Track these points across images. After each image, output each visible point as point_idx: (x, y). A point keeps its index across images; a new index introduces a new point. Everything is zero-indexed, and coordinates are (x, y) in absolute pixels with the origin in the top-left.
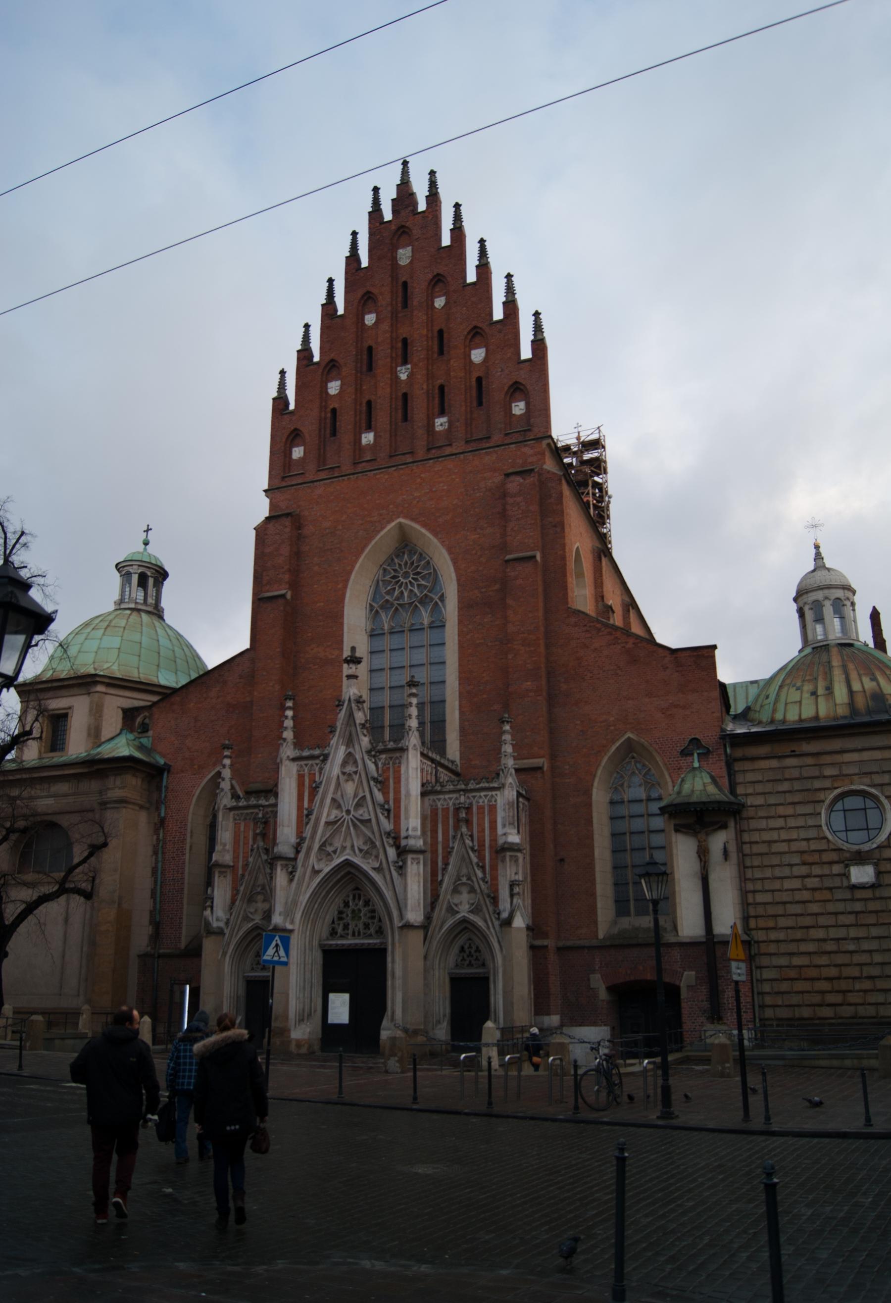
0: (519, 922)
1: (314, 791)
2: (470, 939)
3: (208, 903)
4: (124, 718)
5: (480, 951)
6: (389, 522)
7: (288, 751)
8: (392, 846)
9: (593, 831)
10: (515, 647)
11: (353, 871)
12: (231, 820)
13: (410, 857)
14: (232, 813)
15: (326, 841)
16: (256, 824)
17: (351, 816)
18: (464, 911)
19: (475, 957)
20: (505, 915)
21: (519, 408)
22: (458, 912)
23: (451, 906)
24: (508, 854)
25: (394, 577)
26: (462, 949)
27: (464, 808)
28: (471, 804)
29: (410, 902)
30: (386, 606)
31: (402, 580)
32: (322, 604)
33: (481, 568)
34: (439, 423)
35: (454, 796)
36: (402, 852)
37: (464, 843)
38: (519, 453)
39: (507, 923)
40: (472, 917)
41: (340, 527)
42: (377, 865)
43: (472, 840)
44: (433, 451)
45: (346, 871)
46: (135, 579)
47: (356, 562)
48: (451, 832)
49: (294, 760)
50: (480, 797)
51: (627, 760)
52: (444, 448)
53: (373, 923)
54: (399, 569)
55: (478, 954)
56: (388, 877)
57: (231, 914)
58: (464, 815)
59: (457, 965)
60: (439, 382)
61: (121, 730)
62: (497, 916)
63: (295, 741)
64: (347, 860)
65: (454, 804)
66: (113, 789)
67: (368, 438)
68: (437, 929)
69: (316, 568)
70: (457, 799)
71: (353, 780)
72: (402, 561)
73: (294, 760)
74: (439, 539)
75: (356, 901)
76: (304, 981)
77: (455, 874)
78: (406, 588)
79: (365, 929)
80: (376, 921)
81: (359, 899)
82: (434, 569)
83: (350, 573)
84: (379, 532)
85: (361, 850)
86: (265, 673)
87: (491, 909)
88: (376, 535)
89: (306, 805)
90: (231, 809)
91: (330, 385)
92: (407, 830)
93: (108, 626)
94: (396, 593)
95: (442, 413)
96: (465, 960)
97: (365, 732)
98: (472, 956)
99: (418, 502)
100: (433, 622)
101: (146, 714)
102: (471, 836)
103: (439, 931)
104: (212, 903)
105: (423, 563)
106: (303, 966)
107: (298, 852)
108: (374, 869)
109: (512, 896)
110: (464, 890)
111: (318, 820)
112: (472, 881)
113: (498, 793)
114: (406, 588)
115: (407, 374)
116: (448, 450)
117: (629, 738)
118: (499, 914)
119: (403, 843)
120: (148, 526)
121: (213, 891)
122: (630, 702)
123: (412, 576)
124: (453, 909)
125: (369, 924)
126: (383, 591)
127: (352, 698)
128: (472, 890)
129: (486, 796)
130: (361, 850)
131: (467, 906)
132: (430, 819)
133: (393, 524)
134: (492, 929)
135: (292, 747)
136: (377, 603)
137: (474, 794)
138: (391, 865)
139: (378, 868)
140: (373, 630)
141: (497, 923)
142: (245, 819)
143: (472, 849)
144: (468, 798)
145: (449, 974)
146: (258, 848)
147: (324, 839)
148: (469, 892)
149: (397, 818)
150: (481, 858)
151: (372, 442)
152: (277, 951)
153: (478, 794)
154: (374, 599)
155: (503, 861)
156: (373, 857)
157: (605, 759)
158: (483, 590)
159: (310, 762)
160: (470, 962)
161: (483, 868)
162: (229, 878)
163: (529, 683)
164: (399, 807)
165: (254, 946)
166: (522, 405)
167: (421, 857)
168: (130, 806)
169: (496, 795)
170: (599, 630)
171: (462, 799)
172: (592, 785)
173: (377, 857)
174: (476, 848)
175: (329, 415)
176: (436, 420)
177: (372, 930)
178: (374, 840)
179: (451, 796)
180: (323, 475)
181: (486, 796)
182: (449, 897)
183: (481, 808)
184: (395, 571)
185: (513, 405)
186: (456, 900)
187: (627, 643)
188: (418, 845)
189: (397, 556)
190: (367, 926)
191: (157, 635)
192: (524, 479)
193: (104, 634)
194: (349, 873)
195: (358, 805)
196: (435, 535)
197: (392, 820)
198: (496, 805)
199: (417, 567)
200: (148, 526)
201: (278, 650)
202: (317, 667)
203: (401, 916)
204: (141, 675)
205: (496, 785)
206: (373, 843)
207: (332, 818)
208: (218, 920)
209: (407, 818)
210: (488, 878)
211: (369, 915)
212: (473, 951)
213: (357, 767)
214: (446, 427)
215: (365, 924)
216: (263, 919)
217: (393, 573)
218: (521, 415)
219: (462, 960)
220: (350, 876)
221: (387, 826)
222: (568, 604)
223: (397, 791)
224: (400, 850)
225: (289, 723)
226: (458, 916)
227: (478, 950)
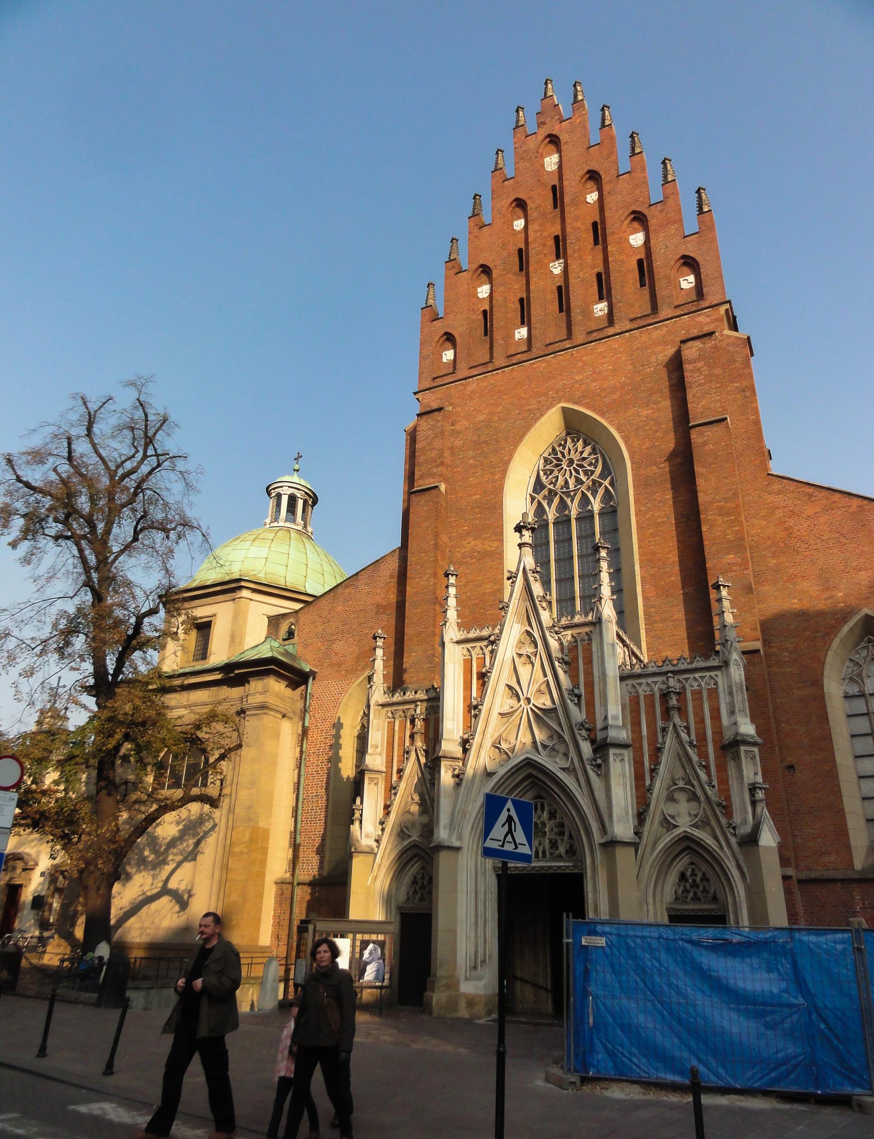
0: (768, 839)
1: (483, 677)
2: (692, 863)
3: (357, 815)
4: (269, 626)
5: (708, 880)
6: (548, 409)
7: (452, 633)
8: (586, 739)
9: (830, 730)
10: (709, 517)
11: (535, 773)
12: (384, 717)
13: (612, 751)
14: (386, 709)
15: (500, 736)
16: (413, 722)
17: (531, 705)
18: (684, 825)
19: (701, 888)
20: (747, 829)
21: (688, 282)
22: (675, 826)
23: (665, 818)
24: (743, 748)
25: (557, 466)
26: (683, 877)
27: (674, 693)
28: (684, 688)
29: (616, 811)
31: (568, 469)
32: (478, 496)
33: (658, 444)
34: (598, 310)
35: (660, 679)
36: (601, 747)
37: (678, 736)
38: (693, 323)
39: (751, 841)
40: (696, 833)
41: (496, 419)
42: (567, 765)
43: (689, 734)
44: (595, 334)
45: (526, 773)
46: (285, 500)
48: (660, 723)
49: (458, 642)
50: (695, 679)
51: (863, 644)
52: (606, 330)
53: (563, 840)
55: (705, 883)
56: (582, 779)
57: (383, 830)
58: (675, 702)
59: (677, 899)
60: (596, 270)
61: (266, 638)
62: (732, 831)
63: (459, 621)
64: (528, 758)
65: (661, 690)
66: (254, 694)
67: (522, 333)
68: (648, 849)
69: (471, 462)
70: (663, 683)
71: (532, 663)
72: (564, 449)
73: (458, 642)
75: (539, 812)
76: (476, 915)
77: (669, 776)
79: (551, 848)
80: (566, 837)
81: (543, 809)
83: (508, 462)
85: (545, 747)
86: (418, 568)
87: (724, 821)
89: (474, 694)
90: (383, 705)
91: (479, 290)
92: (606, 718)
93: (256, 538)
94: (561, 481)
95: (601, 298)
96: (688, 892)
97: (544, 604)
98: (698, 886)
99: (580, 385)
100: (603, 508)
101: (292, 620)
102: (687, 728)
103: (652, 853)
104: (361, 815)
106: (473, 895)
107: (465, 751)
108: (563, 769)
109: (754, 803)
110: (681, 797)
112: (694, 788)
113: (718, 673)
115: (560, 268)
116: (611, 331)
117: (867, 615)
118: (734, 828)
119: (600, 736)
120: (299, 453)
121: (362, 803)
122: (863, 573)
123: (576, 462)
124: (668, 822)
125: (556, 841)
127: (528, 568)
128: (693, 797)
129: (702, 678)
130: (545, 747)
131: (688, 819)
132: (633, 706)
133: (554, 409)
134: (726, 850)
135: (456, 628)
137: (686, 676)
138: (586, 763)
139: (568, 769)
141: (733, 841)
142: (400, 716)
143: (691, 743)
144: (679, 681)
145: (667, 909)
146: (416, 750)
147: (496, 735)
148: (689, 800)
149: (591, 705)
150: (704, 755)
151: (526, 336)
152: (510, 832)
153: (691, 676)
154: (535, 490)
155: (737, 758)
156: (561, 755)
157: (837, 641)
158: (661, 466)
159: (478, 644)
160: (695, 894)
161: (707, 768)
162: (382, 786)
163: (732, 556)
164: (593, 692)
165: (410, 869)
166: (691, 278)
167: (625, 752)
168: (272, 713)
169: (716, 675)
170: (811, 496)
171: (672, 682)
172: (822, 674)
173: (566, 755)
174: (695, 743)
175: (481, 317)
176: (595, 307)
177: (562, 850)
178: (562, 733)
179: (655, 679)
180: (475, 372)
181: (702, 678)
182: (662, 806)
183: (697, 695)
185: (681, 280)
186: (670, 809)
187: (849, 506)
188: (621, 738)
189: (560, 445)
190: (554, 845)
191: (306, 549)
192: (703, 343)
193: (251, 545)
194: (530, 776)
195: (539, 691)
196: (602, 415)
197: (584, 708)
198: (717, 689)
199: (582, 453)
200: (299, 453)
201: (433, 542)
202: (475, 560)
203: (604, 830)
204: (288, 584)
205: (715, 663)
206: (560, 737)
207: (506, 709)
208: (367, 836)
209: (605, 704)
210: (715, 783)
211: (556, 830)
212: (698, 880)
213: (536, 647)
214: (606, 312)
215: (551, 841)
216: (421, 835)
217: (555, 462)
218: (690, 289)
219: (683, 892)
220: (530, 780)
221: (578, 715)
222: (767, 471)
223: (589, 674)
224: (596, 745)
225: (452, 602)
226: (677, 832)
227: (705, 878)
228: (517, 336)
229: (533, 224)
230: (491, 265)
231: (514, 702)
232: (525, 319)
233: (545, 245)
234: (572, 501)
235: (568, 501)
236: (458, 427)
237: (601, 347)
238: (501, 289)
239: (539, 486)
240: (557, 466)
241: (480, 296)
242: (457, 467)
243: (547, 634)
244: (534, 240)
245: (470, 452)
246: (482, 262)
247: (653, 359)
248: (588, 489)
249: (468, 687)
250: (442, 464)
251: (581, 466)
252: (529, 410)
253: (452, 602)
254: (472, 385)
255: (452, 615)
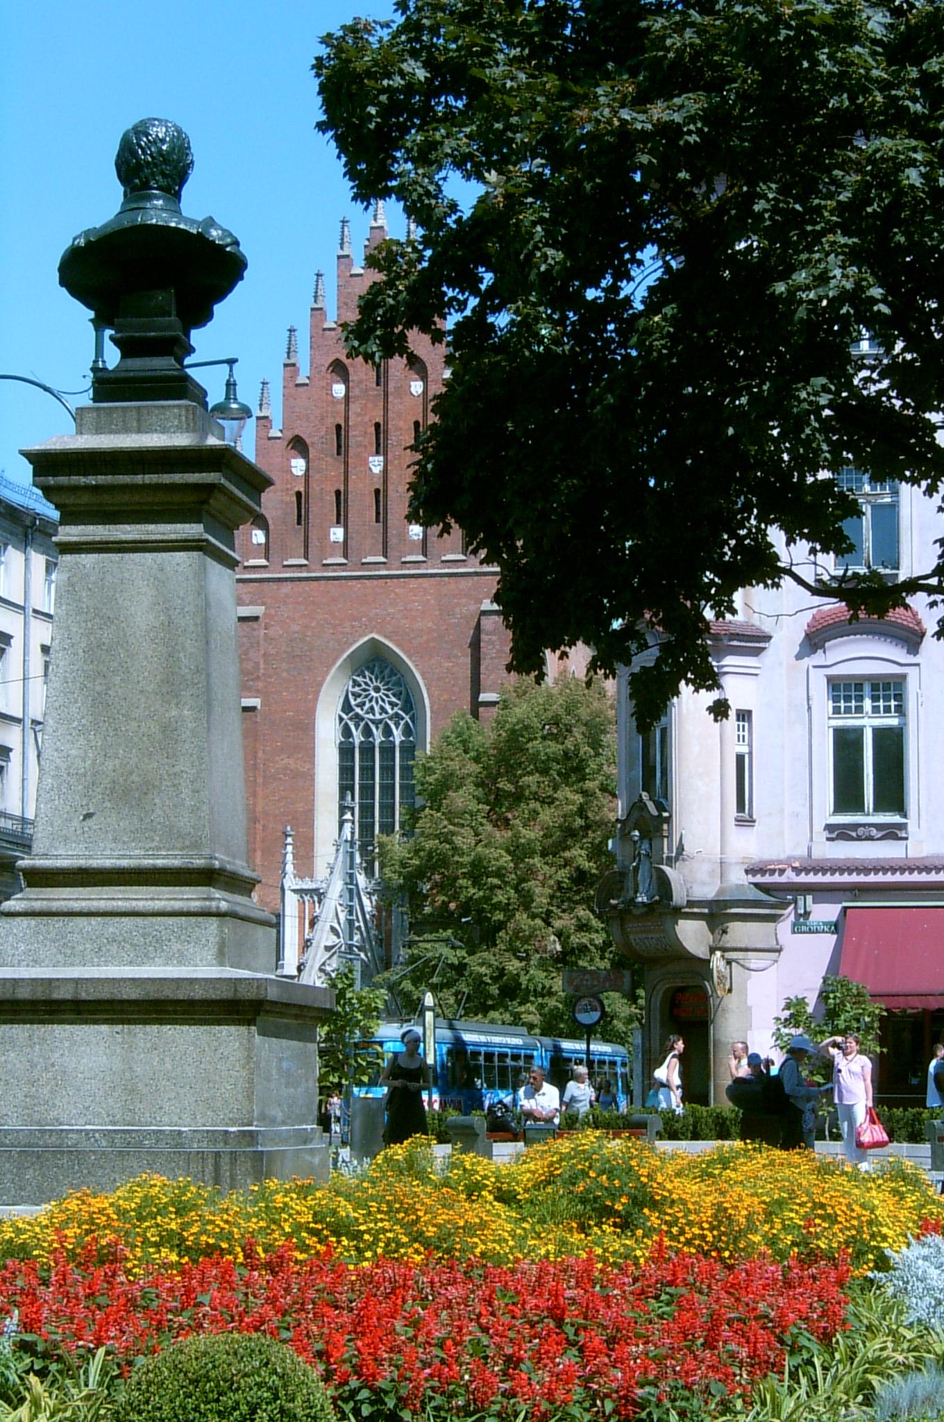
6: (361, 636)
25: (365, 690)
30: (357, 718)
47: (327, 673)
49: (295, 891)
54: (369, 683)
69: (284, 674)
73: (295, 891)
74: (413, 662)
78: (377, 702)
82: (406, 688)
83: (320, 685)
84: (352, 644)
88: (348, 648)
94: (368, 705)
105: (394, 678)
111: (319, 943)
114: (377, 702)
126: (353, 703)
136: (347, 714)
140: (341, 743)
147: (323, 960)
151: (341, 539)
154: (343, 710)
175: (294, 499)
184: (366, 684)
189: (368, 668)
196: (410, 657)
207: (329, 944)
214: (421, 537)
225: (289, 857)
228: (332, 538)
229: (354, 402)
230: (308, 441)
231: (335, 938)
232: (341, 518)
233: (366, 433)
234: (377, 728)
235: (373, 728)
236: (271, 632)
237: (413, 583)
238: (318, 476)
239: (347, 707)
240: (365, 690)
241: (294, 470)
242: (270, 677)
243: (362, 893)
244: (355, 425)
245: (284, 664)
246: (297, 432)
247: (457, 610)
248: (391, 719)
249: (302, 924)
250: (258, 678)
251: (387, 696)
252: (342, 633)
253: (289, 857)
254: (286, 588)
255: (290, 868)
